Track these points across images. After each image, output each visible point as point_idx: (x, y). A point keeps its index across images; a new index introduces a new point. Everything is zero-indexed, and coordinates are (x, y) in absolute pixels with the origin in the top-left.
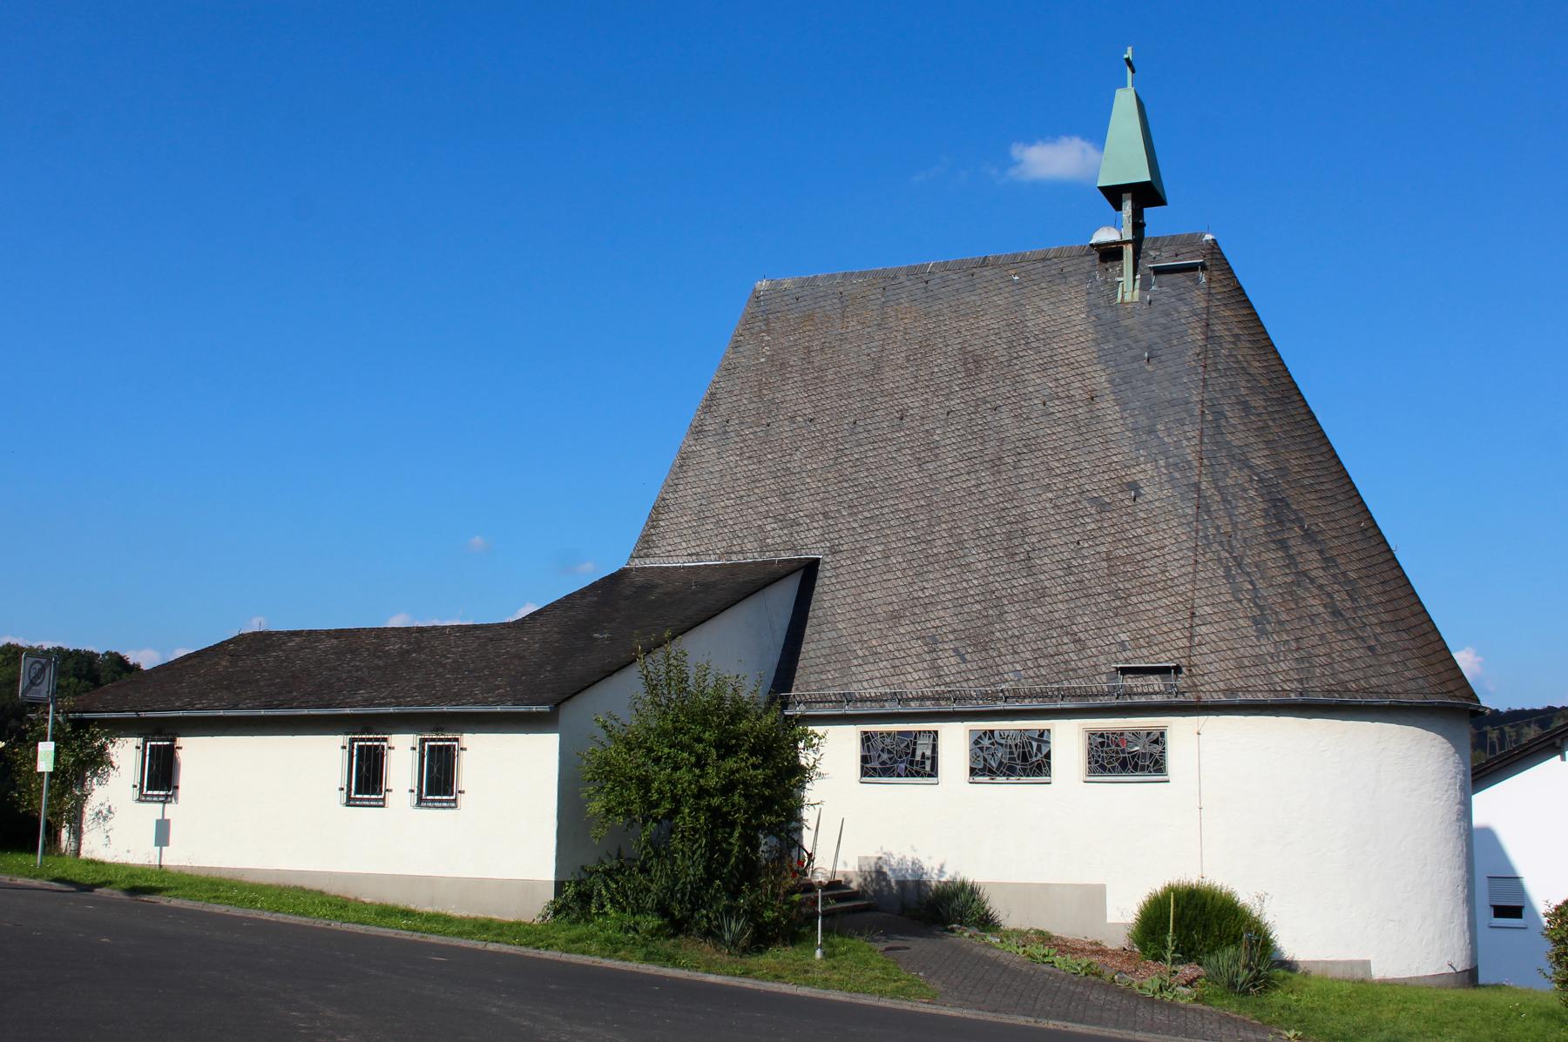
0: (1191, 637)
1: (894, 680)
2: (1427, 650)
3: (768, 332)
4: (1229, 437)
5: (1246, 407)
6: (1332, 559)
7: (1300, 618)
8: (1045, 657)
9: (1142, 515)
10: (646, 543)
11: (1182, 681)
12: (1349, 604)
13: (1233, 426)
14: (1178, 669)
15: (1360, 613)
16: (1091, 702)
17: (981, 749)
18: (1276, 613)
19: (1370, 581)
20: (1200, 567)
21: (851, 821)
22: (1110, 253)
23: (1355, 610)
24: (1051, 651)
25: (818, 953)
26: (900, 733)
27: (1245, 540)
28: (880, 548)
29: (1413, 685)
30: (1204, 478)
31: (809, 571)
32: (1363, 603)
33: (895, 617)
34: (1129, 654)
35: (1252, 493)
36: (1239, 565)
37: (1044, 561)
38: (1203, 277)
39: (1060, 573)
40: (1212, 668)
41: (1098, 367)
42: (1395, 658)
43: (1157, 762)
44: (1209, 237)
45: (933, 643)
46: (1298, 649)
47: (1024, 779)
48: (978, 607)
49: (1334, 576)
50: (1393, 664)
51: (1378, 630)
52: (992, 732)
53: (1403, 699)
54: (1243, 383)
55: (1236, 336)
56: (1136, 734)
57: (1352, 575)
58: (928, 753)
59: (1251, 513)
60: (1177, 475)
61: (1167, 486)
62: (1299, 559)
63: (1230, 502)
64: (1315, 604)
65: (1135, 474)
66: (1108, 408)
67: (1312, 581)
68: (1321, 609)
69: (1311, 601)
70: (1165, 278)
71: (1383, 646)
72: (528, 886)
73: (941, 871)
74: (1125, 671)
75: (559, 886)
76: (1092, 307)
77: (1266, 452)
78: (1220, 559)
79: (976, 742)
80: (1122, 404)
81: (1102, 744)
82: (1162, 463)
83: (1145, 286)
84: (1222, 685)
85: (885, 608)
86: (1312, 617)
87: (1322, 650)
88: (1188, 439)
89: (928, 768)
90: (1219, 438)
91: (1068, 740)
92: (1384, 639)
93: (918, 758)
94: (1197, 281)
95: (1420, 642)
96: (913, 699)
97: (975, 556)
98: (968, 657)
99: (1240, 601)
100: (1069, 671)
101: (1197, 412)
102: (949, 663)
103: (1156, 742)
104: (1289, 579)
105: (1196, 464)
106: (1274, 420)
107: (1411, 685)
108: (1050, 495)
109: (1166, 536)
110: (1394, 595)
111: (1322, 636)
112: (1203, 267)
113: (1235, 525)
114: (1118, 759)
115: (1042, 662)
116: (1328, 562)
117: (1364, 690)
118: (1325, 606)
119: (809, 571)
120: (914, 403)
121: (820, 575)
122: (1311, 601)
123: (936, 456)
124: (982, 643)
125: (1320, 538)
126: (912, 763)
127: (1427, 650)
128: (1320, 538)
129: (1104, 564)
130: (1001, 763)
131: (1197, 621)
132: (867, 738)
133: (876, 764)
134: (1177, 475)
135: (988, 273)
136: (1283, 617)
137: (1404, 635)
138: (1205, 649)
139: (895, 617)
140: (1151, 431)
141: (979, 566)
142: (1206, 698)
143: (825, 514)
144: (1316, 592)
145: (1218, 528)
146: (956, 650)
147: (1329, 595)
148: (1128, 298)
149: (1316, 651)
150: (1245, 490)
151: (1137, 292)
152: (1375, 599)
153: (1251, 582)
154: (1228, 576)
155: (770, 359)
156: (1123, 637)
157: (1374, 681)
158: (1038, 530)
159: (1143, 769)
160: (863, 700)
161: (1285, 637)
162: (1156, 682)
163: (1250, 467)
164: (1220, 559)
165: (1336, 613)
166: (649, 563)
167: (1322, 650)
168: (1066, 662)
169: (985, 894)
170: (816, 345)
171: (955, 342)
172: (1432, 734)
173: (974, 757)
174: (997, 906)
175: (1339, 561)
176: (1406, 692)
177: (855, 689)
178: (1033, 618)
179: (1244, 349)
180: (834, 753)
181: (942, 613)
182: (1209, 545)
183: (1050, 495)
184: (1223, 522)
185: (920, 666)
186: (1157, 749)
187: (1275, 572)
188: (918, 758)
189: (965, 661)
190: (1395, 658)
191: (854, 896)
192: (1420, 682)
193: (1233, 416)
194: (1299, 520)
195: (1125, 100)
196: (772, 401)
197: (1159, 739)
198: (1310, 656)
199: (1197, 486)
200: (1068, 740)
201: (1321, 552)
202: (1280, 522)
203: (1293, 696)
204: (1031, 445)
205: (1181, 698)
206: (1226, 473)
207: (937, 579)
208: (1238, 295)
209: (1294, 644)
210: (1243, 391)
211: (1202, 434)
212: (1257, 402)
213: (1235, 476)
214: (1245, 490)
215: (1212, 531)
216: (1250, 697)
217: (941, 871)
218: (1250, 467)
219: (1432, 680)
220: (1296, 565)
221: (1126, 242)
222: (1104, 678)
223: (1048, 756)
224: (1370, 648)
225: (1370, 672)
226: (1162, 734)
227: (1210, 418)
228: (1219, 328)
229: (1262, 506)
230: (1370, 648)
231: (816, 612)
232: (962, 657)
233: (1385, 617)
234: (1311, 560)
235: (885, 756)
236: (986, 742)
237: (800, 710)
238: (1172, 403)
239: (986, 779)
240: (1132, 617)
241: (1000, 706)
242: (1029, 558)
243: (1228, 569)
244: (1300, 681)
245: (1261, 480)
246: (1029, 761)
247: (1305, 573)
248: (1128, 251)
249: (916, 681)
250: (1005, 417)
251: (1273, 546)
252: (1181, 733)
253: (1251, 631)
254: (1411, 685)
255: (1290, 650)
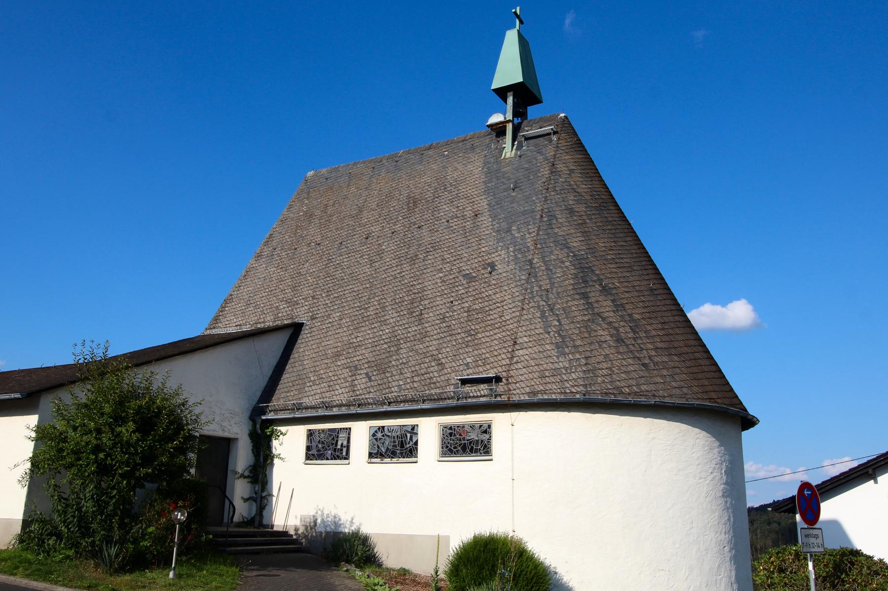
0: (512, 357)
1: (327, 394)
2: (695, 370)
3: (307, 199)
4: (556, 230)
5: (571, 211)
6: (622, 305)
7: (591, 344)
8: (418, 375)
9: (494, 282)
10: (216, 320)
11: (501, 388)
12: (631, 335)
13: (561, 223)
14: (498, 379)
15: (639, 341)
16: (442, 404)
17: (376, 439)
18: (574, 340)
19: (652, 321)
20: (525, 312)
21: (303, 491)
22: (499, 130)
23: (634, 339)
24: (423, 371)
25: (171, 575)
26: (330, 430)
27: (558, 293)
28: (338, 314)
29: (674, 387)
30: (536, 256)
31: (296, 329)
32: (643, 334)
33: (337, 355)
34: (470, 371)
35: (567, 264)
36: (552, 310)
37: (430, 316)
38: (555, 138)
39: (438, 322)
40: (522, 378)
41: (483, 197)
42: (665, 372)
43: (486, 446)
44: (562, 115)
45: (354, 369)
46: (586, 364)
47: (401, 460)
48: (385, 346)
49: (621, 316)
50: (662, 376)
51: (653, 353)
52: (383, 427)
53: (667, 400)
54: (572, 198)
55: (572, 171)
56: (472, 427)
57: (637, 316)
58: (345, 443)
59: (564, 275)
60: (520, 256)
61: (512, 263)
62: (595, 305)
63: (551, 270)
64: (604, 334)
65: (494, 258)
66: (485, 220)
67: (604, 319)
68: (608, 338)
69: (601, 332)
70: (531, 141)
71: (656, 364)
72: (9, 522)
73: (352, 522)
74: (464, 382)
75: (26, 523)
76: (486, 163)
77: (581, 239)
78: (538, 307)
79: (374, 435)
80: (494, 217)
81: (451, 434)
82: (511, 249)
83: (520, 147)
84: (528, 390)
85: (333, 350)
86: (600, 343)
87: (605, 365)
88: (530, 233)
89: (344, 453)
90: (549, 231)
91: (429, 431)
92: (656, 359)
93: (339, 447)
94: (551, 141)
95: (688, 364)
96: (335, 406)
97: (391, 316)
98: (373, 378)
99: (549, 333)
100: (431, 383)
101: (538, 217)
102: (361, 382)
103: (485, 432)
104: (586, 318)
105: (532, 248)
106: (590, 219)
107: (677, 392)
108: (441, 275)
109: (506, 295)
110: (671, 331)
111: (606, 356)
112: (555, 133)
113: (552, 284)
114: (465, 445)
115: (416, 379)
116: (618, 307)
117: (635, 393)
118: (611, 336)
119: (296, 329)
120: (376, 229)
121: (302, 332)
122: (601, 332)
123: (381, 258)
124: (381, 367)
125: (614, 291)
126: (335, 450)
127: (695, 370)
128: (614, 291)
129: (466, 314)
130: (388, 449)
131: (517, 347)
132: (310, 434)
133: (314, 452)
134: (520, 256)
135: (431, 152)
136: (578, 343)
137: (676, 358)
138: (520, 365)
139: (337, 355)
140: (509, 230)
141: (392, 321)
142: (515, 398)
143: (313, 297)
144: (606, 326)
145: (540, 287)
146: (367, 374)
147: (615, 328)
148: (508, 156)
149: (601, 366)
150: (563, 262)
151: (514, 151)
152: (654, 333)
153: (559, 321)
154: (543, 316)
155: (306, 213)
156: (469, 360)
157: (644, 388)
158: (429, 296)
159: (476, 451)
160: (307, 408)
161: (578, 356)
162: (483, 388)
163: (568, 248)
164: (538, 307)
165: (619, 340)
166: (214, 332)
167: (605, 365)
168: (431, 378)
169: (374, 540)
170: (331, 202)
171: (405, 193)
172: (697, 430)
173: (372, 446)
174: (381, 550)
175: (627, 307)
176: (671, 396)
177: (307, 401)
178: (416, 351)
179: (577, 177)
180: (290, 443)
181: (364, 351)
182: (533, 297)
183: (441, 275)
184: (546, 284)
185: (344, 385)
186: (485, 437)
187: (577, 313)
188: (339, 447)
189: (370, 380)
190: (665, 372)
191: (295, 542)
192: (685, 390)
193: (562, 218)
194: (600, 281)
195: (511, 39)
196: (301, 236)
197: (487, 430)
198: (595, 369)
199: (531, 262)
200: (429, 431)
201: (613, 301)
202: (585, 282)
203: (578, 396)
204: (435, 246)
205: (499, 399)
206: (551, 252)
207: (366, 331)
208: (579, 147)
209: (583, 361)
210: (571, 202)
211: (538, 231)
212: (581, 208)
213: (558, 253)
214: (563, 262)
215: (536, 288)
216: (546, 397)
217: (352, 522)
218: (568, 248)
219: (695, 389)
220: (593, 309)
221: (509, 121)
222: (452, 387)
223: (416, 443)
224: (644, 365)
225: (642, 381)
226: (489, 426)
227: (545, 219)
228: (560, 166)
229: (573, 271)
230: (644, 365)
231: (295, 355)
232: (370, 380)
233: (659, 345)
234: (605, 306)
235: (320, 446)
236: (379, 435)
237: (271, 416)
238: (524, 213)
239: (378, 460)
240: (476, 347)
241: (386, 408)
242: (421, 314)
243: (543, 312)
244: (585, 386)
245: (575, 256)
246: (401, 448)
247: (599, 314)
248: (509, 127)
249: (341, 395)
250: (425, 231)
251: (577, 297)
252: (502, 424)
253: (554, 353)
254: (677, 392)
255: (580, 365)
